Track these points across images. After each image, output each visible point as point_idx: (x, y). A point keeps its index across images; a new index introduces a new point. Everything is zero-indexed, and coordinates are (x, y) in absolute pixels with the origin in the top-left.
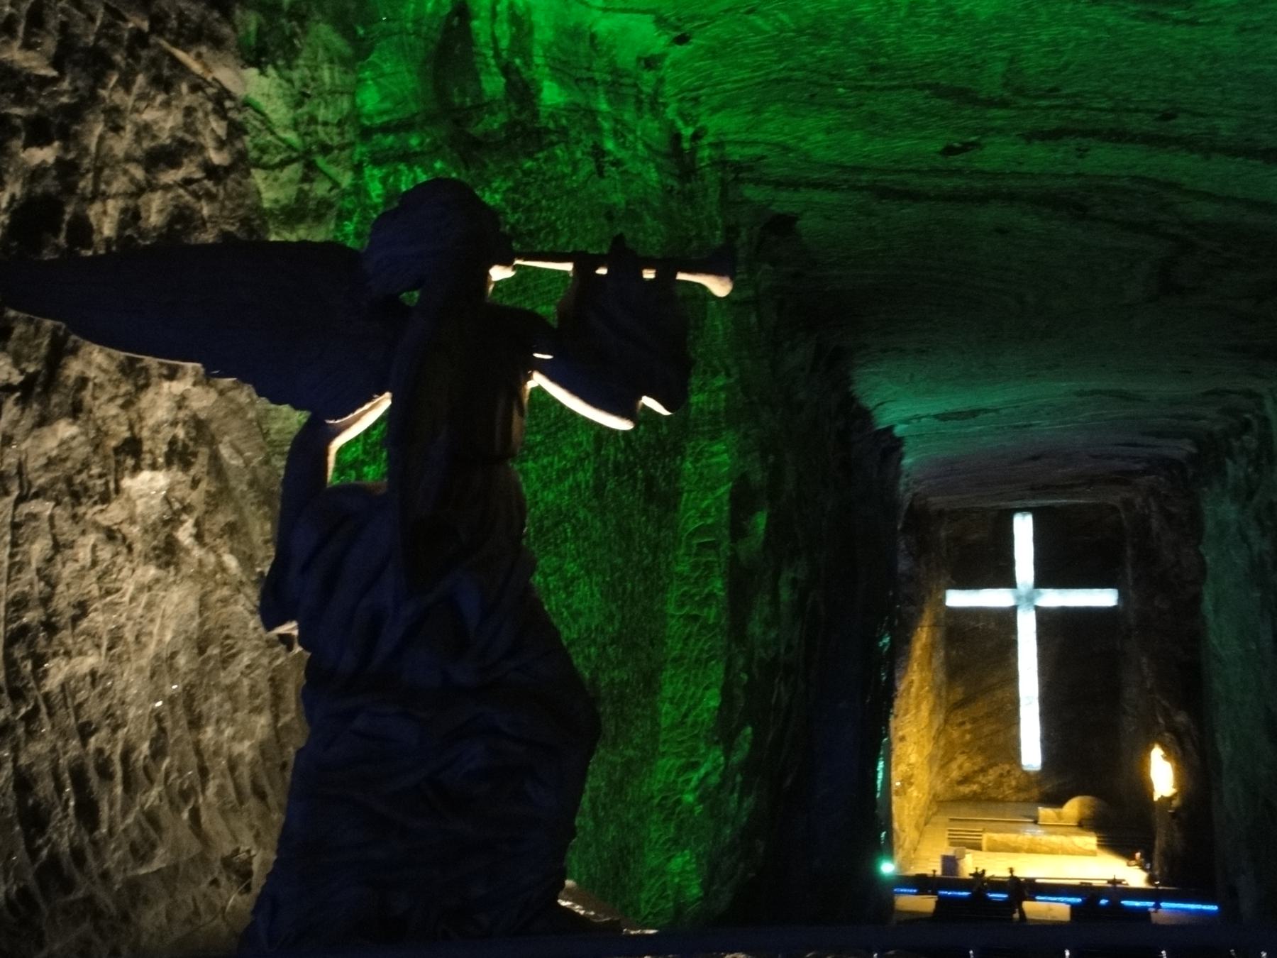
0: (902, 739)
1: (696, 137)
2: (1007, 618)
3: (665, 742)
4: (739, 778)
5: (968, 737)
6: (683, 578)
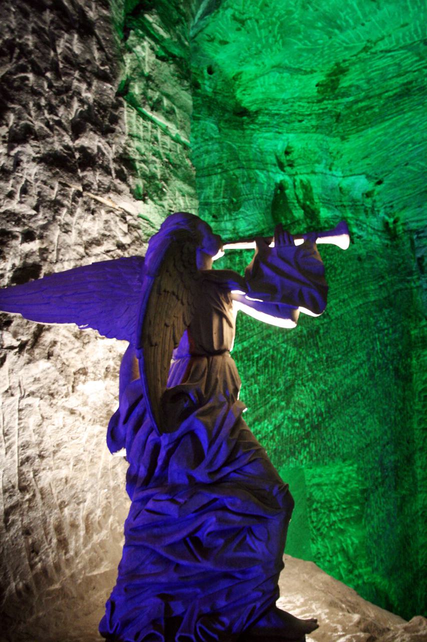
1: (395, 222)
3: (421, 486)
6: (419, 412)
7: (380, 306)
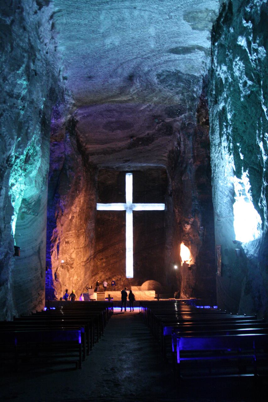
2: (122, 214)
5: (104, 265)
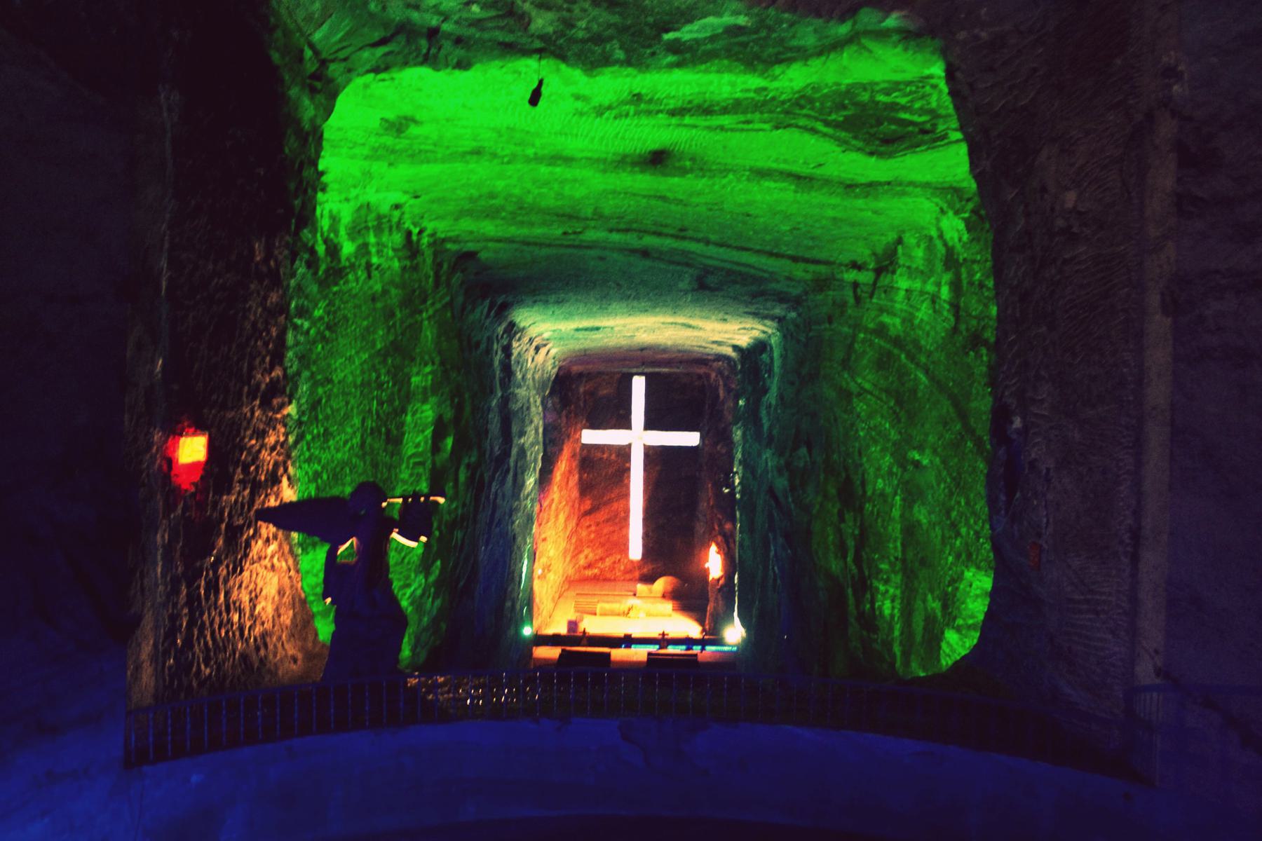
0: (544, 540)
1: (421, 232)
4: (432, 590)
6: (404, 482)
7: (384, 355)
